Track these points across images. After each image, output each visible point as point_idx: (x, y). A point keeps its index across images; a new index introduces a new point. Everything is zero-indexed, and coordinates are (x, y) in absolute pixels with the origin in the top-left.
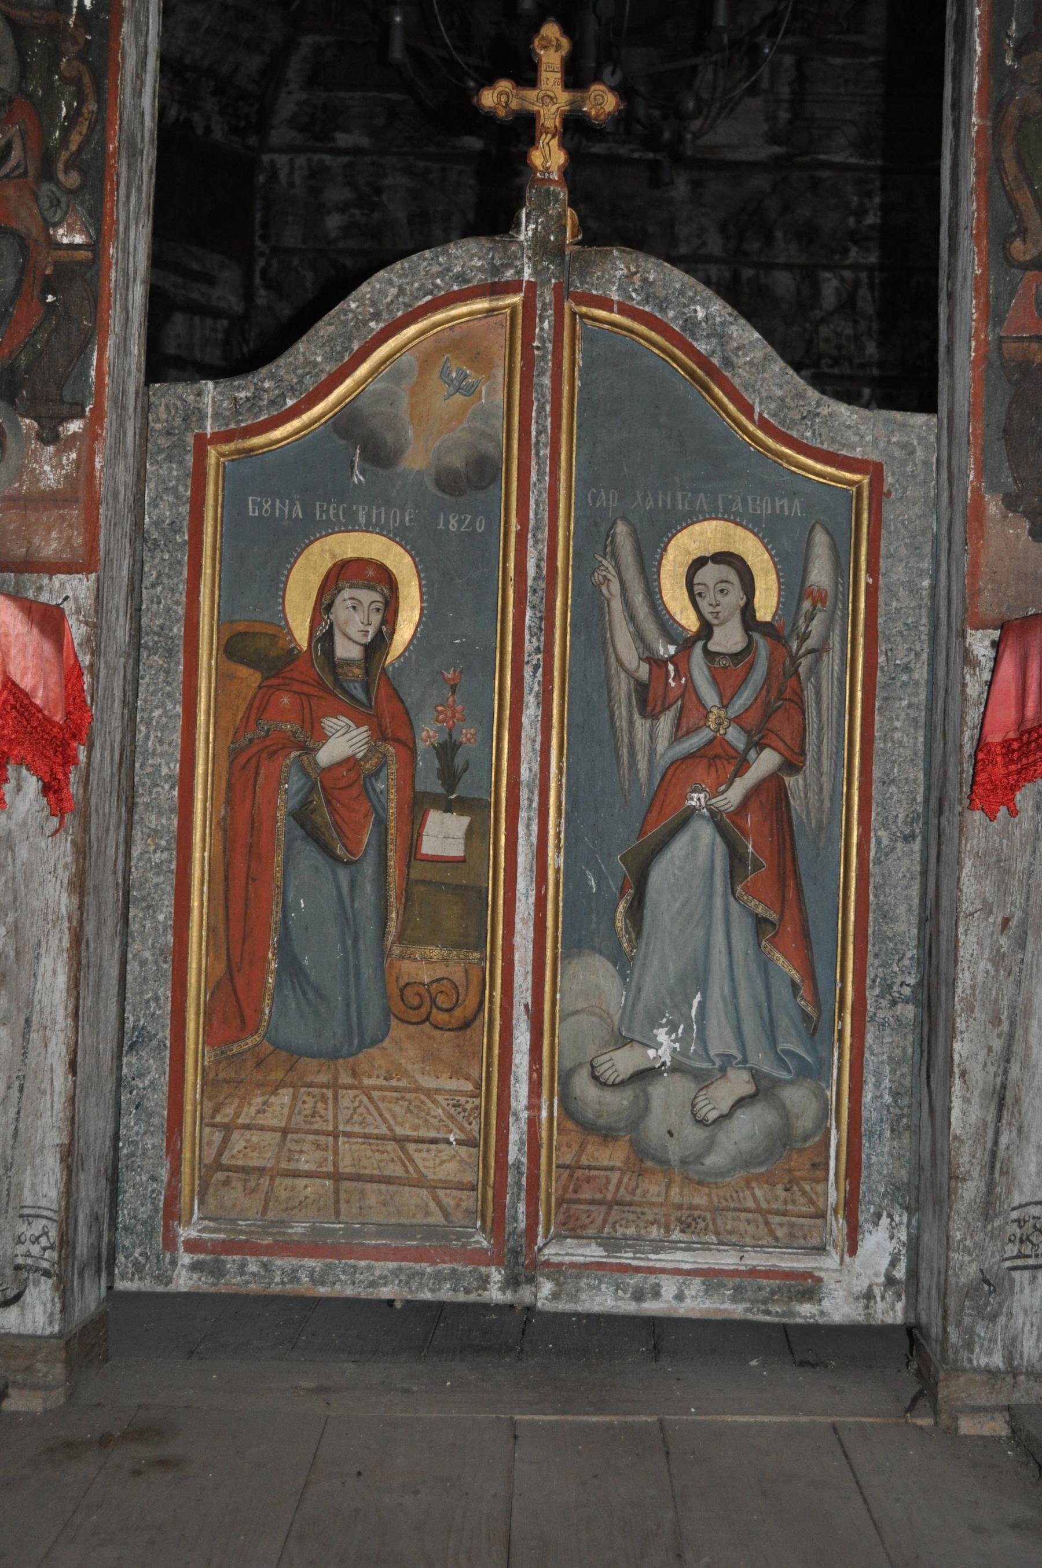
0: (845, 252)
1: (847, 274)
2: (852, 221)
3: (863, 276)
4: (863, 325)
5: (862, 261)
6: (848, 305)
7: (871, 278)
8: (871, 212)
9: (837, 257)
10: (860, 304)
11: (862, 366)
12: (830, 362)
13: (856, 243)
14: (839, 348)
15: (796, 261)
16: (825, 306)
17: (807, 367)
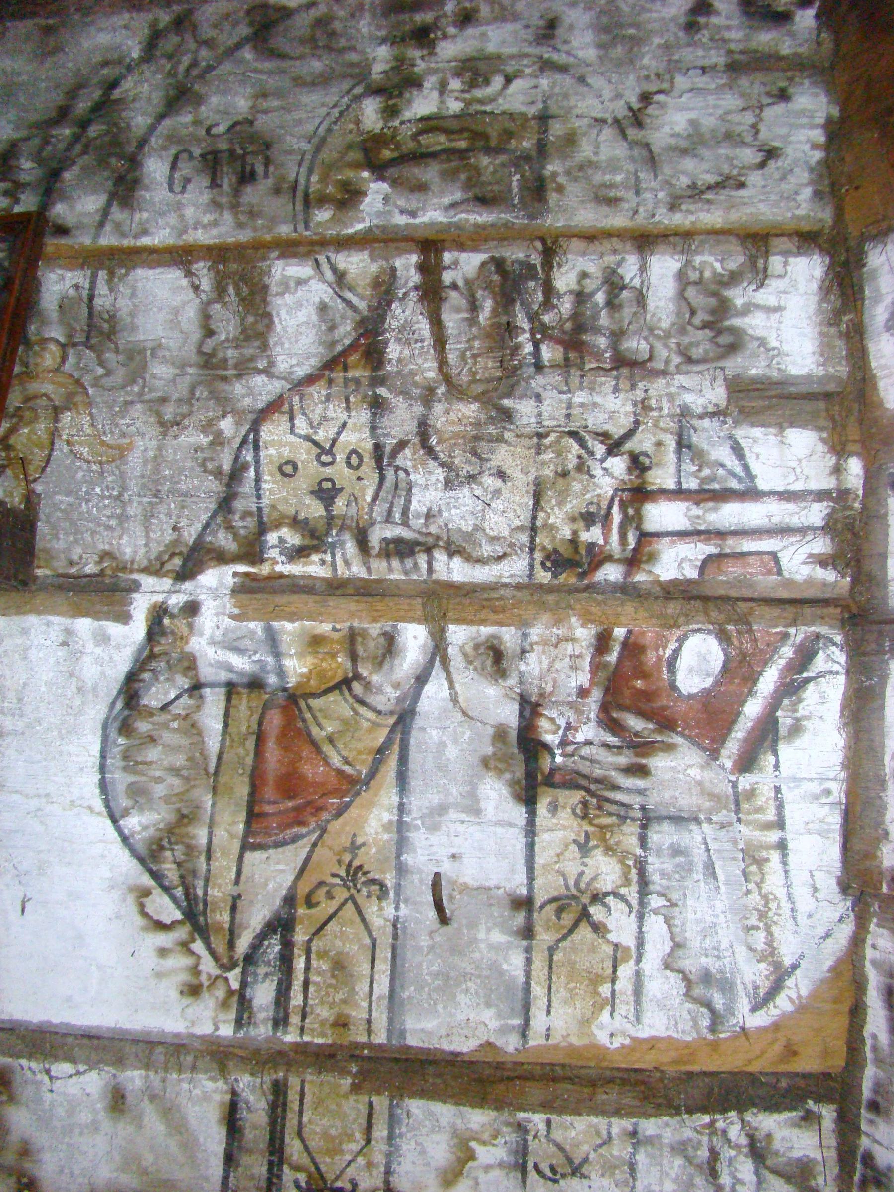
0: (349, 197)
1: (356, 264)
2: (370, 113)
3: (407, 264)
4: (401, 419)
5: (401, 220)
6: (358, 356)
7: (430, 270)
8: (430, 82)
9: (323, 215)
10: (394, 351)
11: (400, 549)
12: (293, 539)
13: (379, 170)
14: (326, 493)
15: (201, 237)
16: (282, 364)
17: (222, 558)
